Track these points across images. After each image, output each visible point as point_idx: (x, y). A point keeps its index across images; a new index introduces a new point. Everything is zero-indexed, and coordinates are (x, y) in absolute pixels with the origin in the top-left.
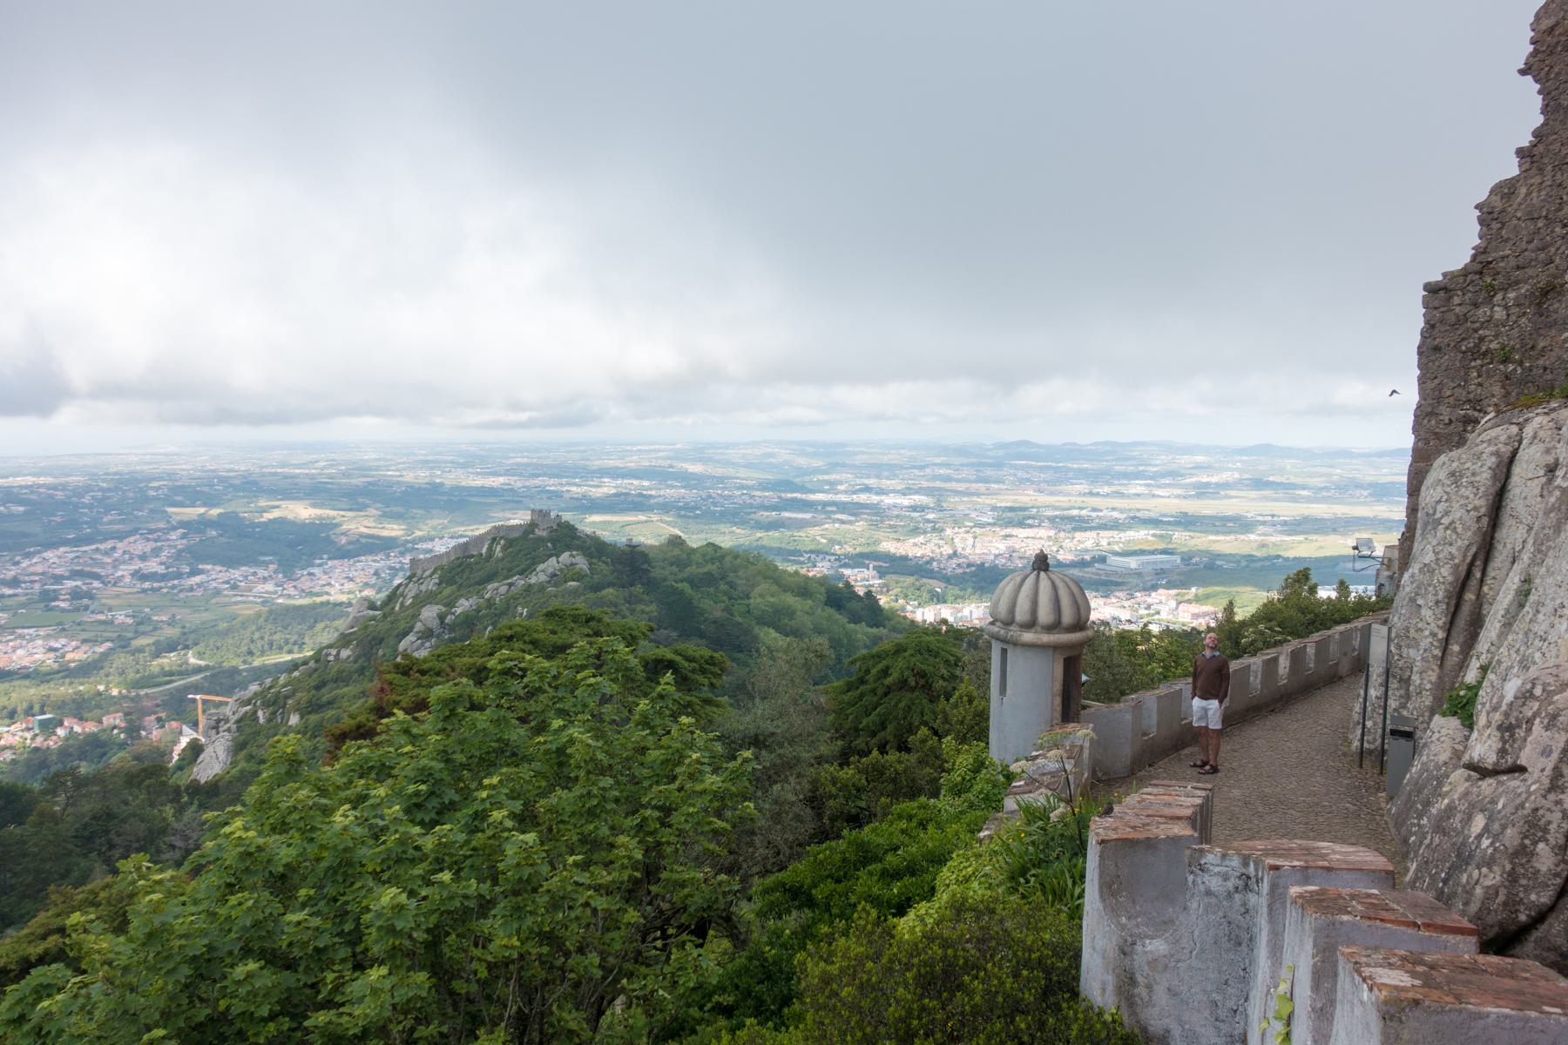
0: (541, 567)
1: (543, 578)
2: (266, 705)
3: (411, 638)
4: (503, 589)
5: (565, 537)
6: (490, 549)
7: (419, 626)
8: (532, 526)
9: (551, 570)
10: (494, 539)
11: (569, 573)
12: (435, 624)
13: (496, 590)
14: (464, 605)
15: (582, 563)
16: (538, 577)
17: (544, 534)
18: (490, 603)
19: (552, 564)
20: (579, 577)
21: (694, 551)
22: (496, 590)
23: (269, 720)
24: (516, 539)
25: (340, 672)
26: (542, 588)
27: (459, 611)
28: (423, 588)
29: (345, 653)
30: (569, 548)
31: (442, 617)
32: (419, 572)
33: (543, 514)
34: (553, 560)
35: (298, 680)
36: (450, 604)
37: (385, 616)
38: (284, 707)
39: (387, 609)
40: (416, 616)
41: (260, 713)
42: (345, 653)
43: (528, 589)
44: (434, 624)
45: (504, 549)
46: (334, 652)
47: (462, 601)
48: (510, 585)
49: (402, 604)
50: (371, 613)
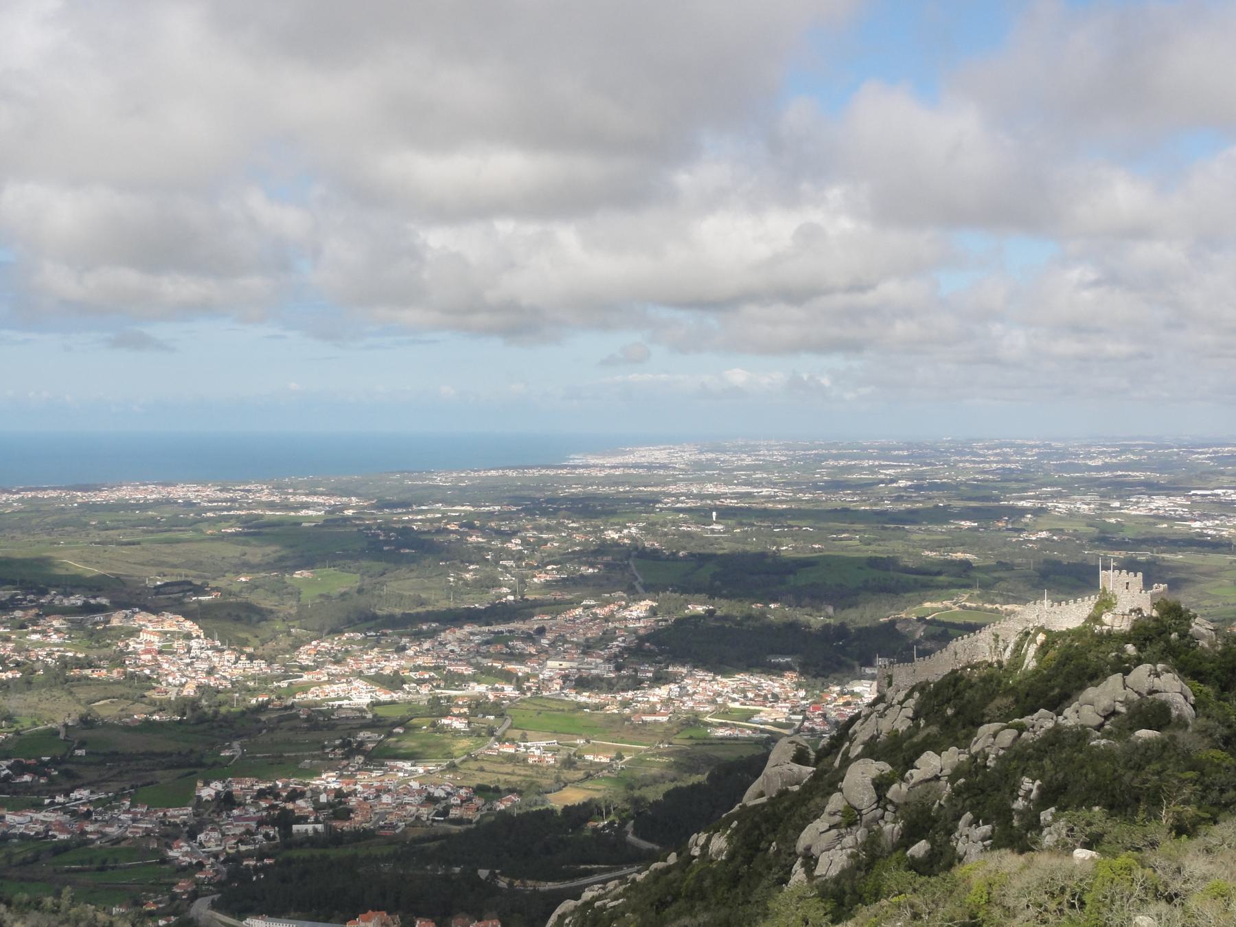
0: (1090, 692)
3: (820, 824)
4: (1008, 736)
7: (835, 802)
9: (1105, 703)
11: (1153, 713)
13: (993, 739)
15: (1172, 688)
19: (1109, 693)
22: (993, 739)
24: (1069, 633)
25: (700, 878)
26: (1081, 735)
28: (885, 725)
31: (881, 785)
32: (890, 693)
34: (1115, 680)
37: (816, 777)
39: (821, 765)
42: (719, 843)
48: (1021, 729)
50: (796, 767)
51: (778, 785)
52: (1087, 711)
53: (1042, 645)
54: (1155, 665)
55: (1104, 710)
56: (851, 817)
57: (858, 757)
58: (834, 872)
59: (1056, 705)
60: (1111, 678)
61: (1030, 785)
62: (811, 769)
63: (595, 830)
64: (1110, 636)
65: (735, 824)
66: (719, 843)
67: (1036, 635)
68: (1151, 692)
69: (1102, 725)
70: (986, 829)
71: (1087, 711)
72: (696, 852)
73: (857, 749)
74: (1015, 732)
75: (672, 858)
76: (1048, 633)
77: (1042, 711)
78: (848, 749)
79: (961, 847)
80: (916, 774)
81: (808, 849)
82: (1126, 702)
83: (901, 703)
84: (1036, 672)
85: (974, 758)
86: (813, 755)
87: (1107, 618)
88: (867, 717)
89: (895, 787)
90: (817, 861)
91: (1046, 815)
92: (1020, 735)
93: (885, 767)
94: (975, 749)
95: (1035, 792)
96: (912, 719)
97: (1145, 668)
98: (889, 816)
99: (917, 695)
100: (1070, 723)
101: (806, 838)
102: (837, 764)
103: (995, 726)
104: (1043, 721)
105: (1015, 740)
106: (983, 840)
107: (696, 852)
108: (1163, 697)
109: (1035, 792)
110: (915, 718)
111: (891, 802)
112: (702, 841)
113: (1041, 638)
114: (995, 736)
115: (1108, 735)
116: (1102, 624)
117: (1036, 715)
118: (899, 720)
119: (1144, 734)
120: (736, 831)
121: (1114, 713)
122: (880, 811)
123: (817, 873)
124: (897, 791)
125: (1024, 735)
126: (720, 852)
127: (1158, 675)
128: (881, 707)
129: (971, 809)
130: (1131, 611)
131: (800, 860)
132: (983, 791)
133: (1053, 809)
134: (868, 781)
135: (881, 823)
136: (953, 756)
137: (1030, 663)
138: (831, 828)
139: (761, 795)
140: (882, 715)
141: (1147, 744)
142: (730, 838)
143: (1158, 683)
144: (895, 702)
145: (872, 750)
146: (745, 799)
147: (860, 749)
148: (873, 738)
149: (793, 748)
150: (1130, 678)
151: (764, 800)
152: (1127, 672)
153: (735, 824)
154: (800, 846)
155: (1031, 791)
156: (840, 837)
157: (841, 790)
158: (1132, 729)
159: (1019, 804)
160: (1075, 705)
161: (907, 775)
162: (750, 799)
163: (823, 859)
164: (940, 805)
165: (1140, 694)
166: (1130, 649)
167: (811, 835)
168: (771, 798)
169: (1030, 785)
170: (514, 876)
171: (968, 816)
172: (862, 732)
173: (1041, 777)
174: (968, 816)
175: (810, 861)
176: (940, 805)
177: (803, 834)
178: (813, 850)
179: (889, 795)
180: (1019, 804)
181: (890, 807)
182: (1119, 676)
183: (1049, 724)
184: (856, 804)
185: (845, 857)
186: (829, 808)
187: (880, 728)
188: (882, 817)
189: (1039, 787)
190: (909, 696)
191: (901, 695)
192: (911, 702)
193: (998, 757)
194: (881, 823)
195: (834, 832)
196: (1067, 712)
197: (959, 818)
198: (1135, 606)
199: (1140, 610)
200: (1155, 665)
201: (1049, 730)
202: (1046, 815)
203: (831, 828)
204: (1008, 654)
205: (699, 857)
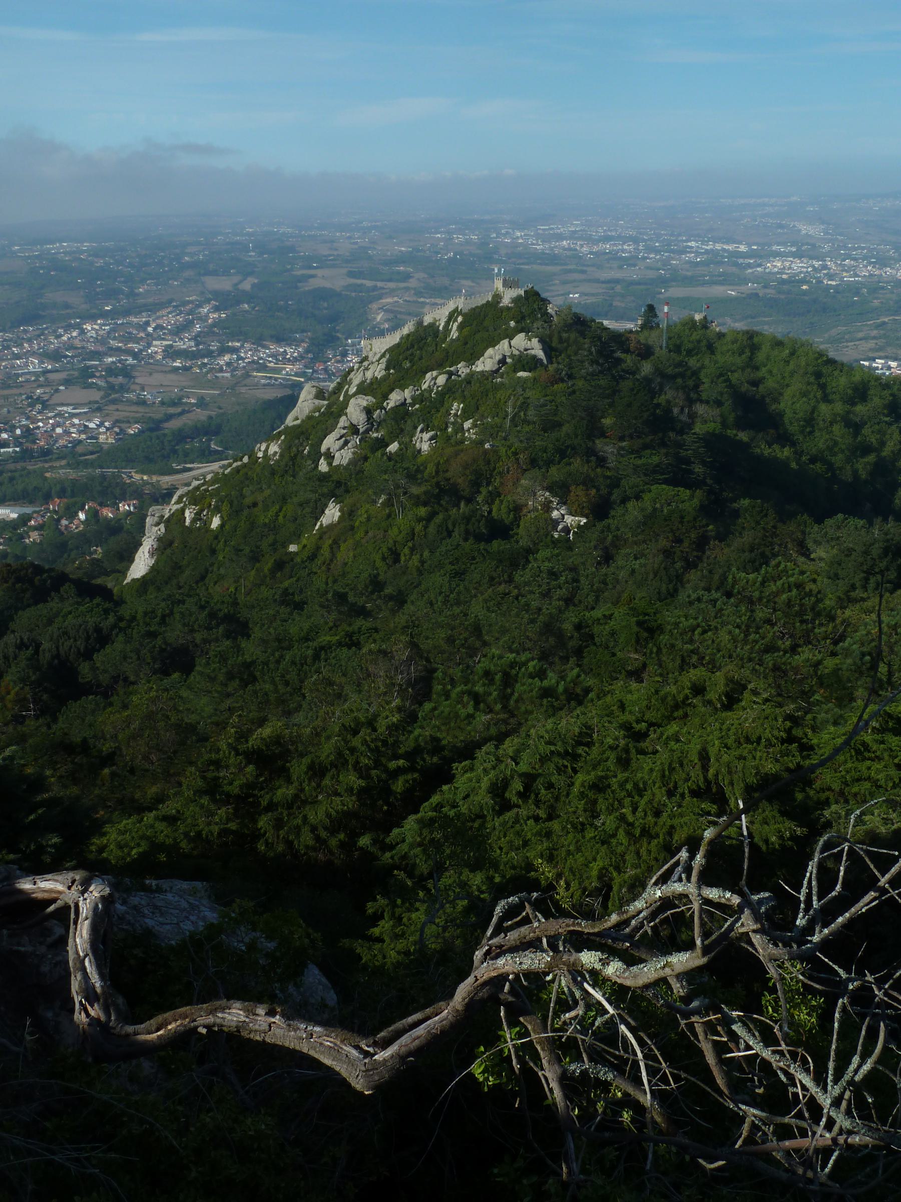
0: (490, 351)
11: (525, 361)
14: (395, 398)
16: (486, 363)
28: (369, 375)
31: (368, 411)
32: (371, 355)
34: (506, 342)
36: (386, 397)
37: (329, 406)
39: (333, 398)
40: (342, 410)
42: (274, 448)
43: (470, 379)
45: (461, 327)
48: (450, 374)
50: (317, 402)
51: (306, 412)
56: (353, 429)
57: (354, 395)
58: (345, 462)
61: (457, 407)
62: (326, 402)
65: (283, 437)
66: (274, 448)
67: (457, 317)
68: (526, 350)
73: (353, 390)
75: (246, 459)
78: (347, 390)
81: (329, 449)
82: (512, 356)
83: (378, 361)
84: (458, 338)
88: (358, 370)
90: (334, 457)
91: (467, 425)
97: (522, 335)
100: (478, 370)
102: (341, 398)
103: (435, 373)
104: (462, 369)
105: (447, 380)
107: (260, 455)
108: (533, 352)
110: (387, 368)
112: (263, 448)
113: (460, 319)
114: (436, 378)
117: (459, 366)
118: (377, 371)
119: (521, 374)
120: (283, 441)
123: (334, 464)
126: (276, 453)
128: (366, 363)
129: (424, 421)
137: (454, 334)
140: (367, 369)
141: (526, 380)
142: (280, 446)
145: (363, 389)
147: (355, 389)
148: (363, 382)
149: (314, 390)
150: (513, 342)
151: (298, 422)
152: (511, 339)
153: (283, 437)
154: (323, 449)
156: (346, 443)
157: (346, 414)
158: (516, 371)
160: (481, 359)
162: (290, 421)
163: (337, 455)
167: (330, 442)
168: (303, 421)
169: (457, 407)
170: (143, 473)
172: (356, 379)
175: (329, 456)
177: (325, 442)
182: (506, 341)
184: (355, 422)
186: (339, 426)
190: (383, 356)
192: (384, 360)
197: (416, 428)
202: (467, 425)
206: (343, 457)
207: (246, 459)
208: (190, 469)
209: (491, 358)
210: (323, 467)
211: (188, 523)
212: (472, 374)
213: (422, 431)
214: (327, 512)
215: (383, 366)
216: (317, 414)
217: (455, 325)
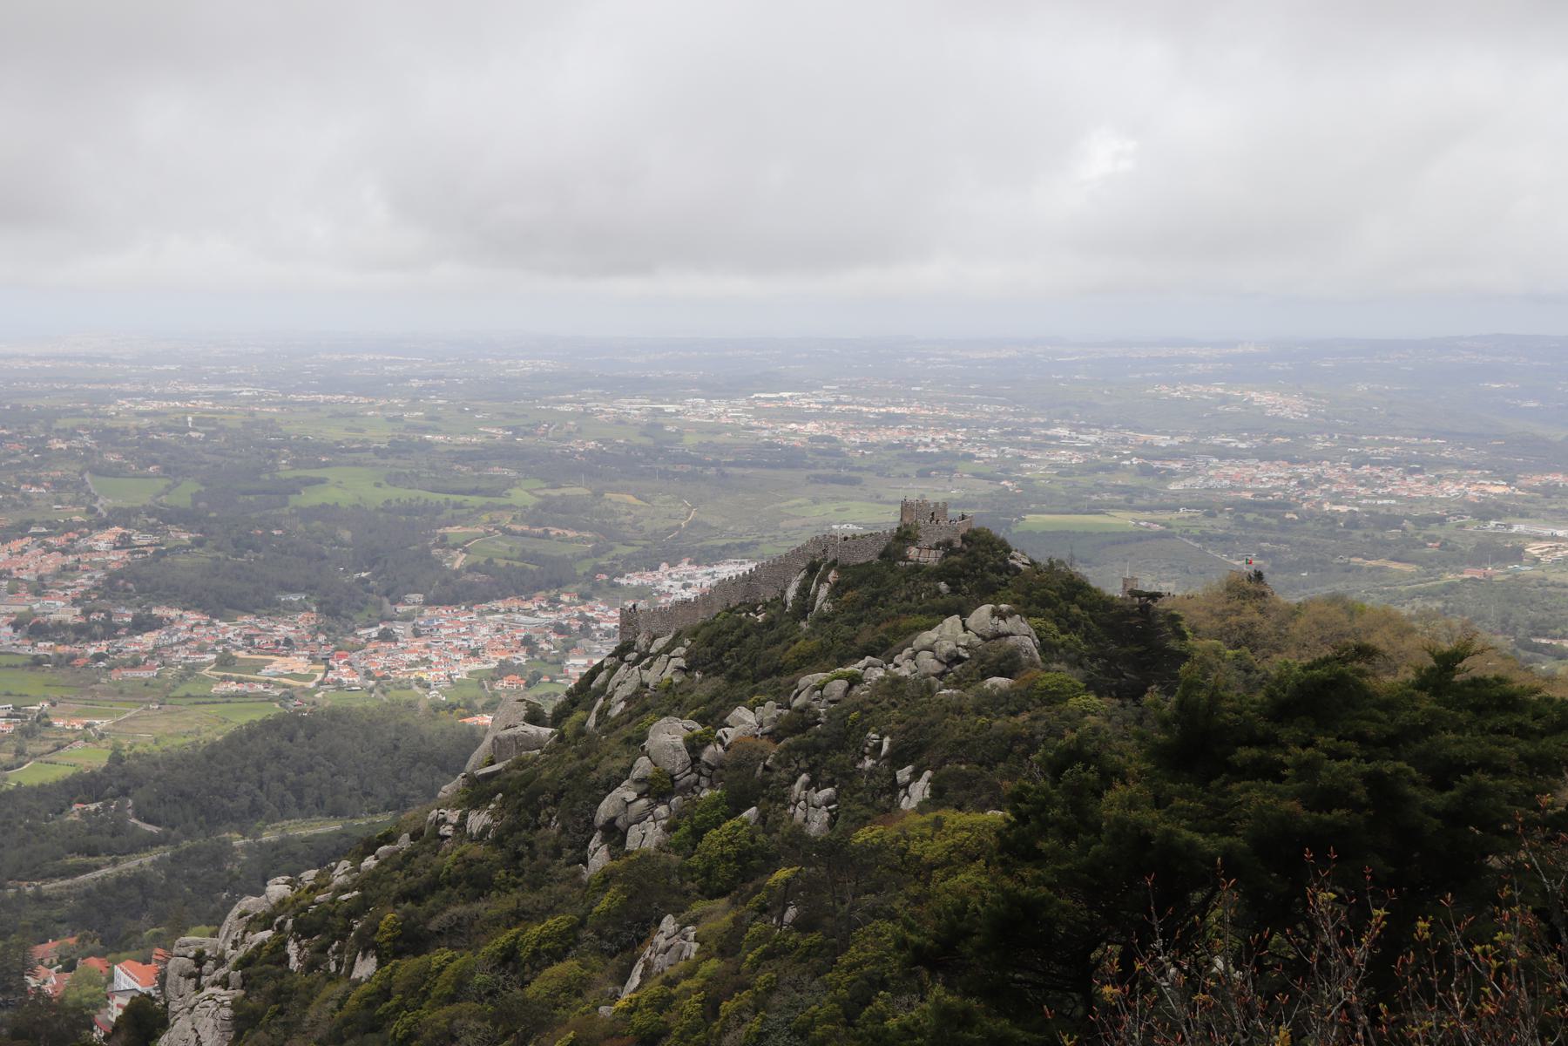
0: (927, 637)
1: (928, 662)
2: (304, 930)
5: (977, 565)
6: (803, 590)
7: (643, 766)
8: (905, 536)
9: (947, 647)
10: (813, 569)
12: (678, 761)
13: (819, 688)
15: (1022, 633)
17: (932, 558)
18: (801, 722)
19: (949, 634)
20: (1009, 665)
21: (1294, 613)
22: (819, 688)
23: (310, 966)
27: (731, 734)
28: (651, 677)
29: (477, 821)
30: (987, 592)
31: (694, 746)
32: (642, 641)
33: (935, 514)
35: (374, 876)
38: (343, 938)
39: (569, 726)
41: (292, 949)
42: (477, 821)
44: (678, 761)
45: (837, 591)
46: (453, 816)
47: (741, 712)
48: (854, 680)
49: (602, 713)
50: (532, 729)
52: (925, 657)
53: (837, 584)
54: (996, 604)
55: (948, 656)
58: (650, 844)
59: (882, 649)
60: (948, 621)
62: (549, 730)
63: (83, 814)
64: (917, 568)
68: (998, 636)
69: (944, 673)
70: (828, 792)
71: (925, 657)
72: (446, 830)
74: (845, 683)
76: (843, 569)
77: (868, 658)
79: (799, 815)
80: (731, 734)
81: (613, 820)
83: (667, 649)
85: (801, 711)
86: (548, 711)
87: (913, 552)
89: (711, 748)
90: (624, 835)
92: (851, 687)
93: (698, 729)
94: (797, 703)
95: (885, 747)
96: (685, 671)
97: (986, 609)
98: (704, 782)
99: (688, 642)
100: (904, 672)
101: (606, 808)
102: (591, 722)
106: (827, 805)
109: (885, 747)
111: (708, 766)
115: (957, 683)
116: (905, 559)
117: (862, 663)
121: (959, 660)
122: (695, 776)
124: (710, 753)
125: (856, 689)
126: (486, 829)
127: (1003, 616)
128: (632, 656)
129: (809, 770)
130: (938, 546)
131: (598, 836)
132: (817, 749)
133: (909, 768)
134: (679, 741)
135: (697, 789)
136: (770, 710)
138: (640, 796)
139: (492, 763)
142: (492, 814)
143: (1004, 626)
144: (652, 650)
146: (468, 768)
149: (523, 706)
150: (971, 621)
152: (964, 614)
155: (880, 746)
156: (651, 807)
159: (869, 763)
160: (908, 651)
161: (719, 733)
163: (634, 833)
164: (766, 768)
165: (984, 638)
166: (943, 586)
171: (804, 777)
173: (892, 734)
174: (804, 777)
175: (614, 834)
176: (766, 768)
177: (603, 806)
178: (619, 822)
179: (704, 757)
180: (869, 763)
181: (704, 771)
183: (880, 673)
185: (659, 829)
186: (635, 774)
187: (646, 680)
188: (697, 783)
189: (890, 744)
191: (660, 643)
192: (682, 650)
193: (829, 715)
194: (697, 789)
195: (643, 802)
196: (897, 659)
198: (943, 538)
199: (949, 544)
200: (996, 604)
201: (882, 679)
202: (903, 775)
203: (640, 796)
204: (791, 593)
205: (454, 838)
206: (646, 836)
207: (404, 842)
208: (86, 869)
209: (930, 649)
210: (599, 858)
211: (294, 964)
212: (898, 681)
213: (807, 787)
214: (660, 941)
215: (682, 663)
216: (537, 752)
217: (824, 591)
